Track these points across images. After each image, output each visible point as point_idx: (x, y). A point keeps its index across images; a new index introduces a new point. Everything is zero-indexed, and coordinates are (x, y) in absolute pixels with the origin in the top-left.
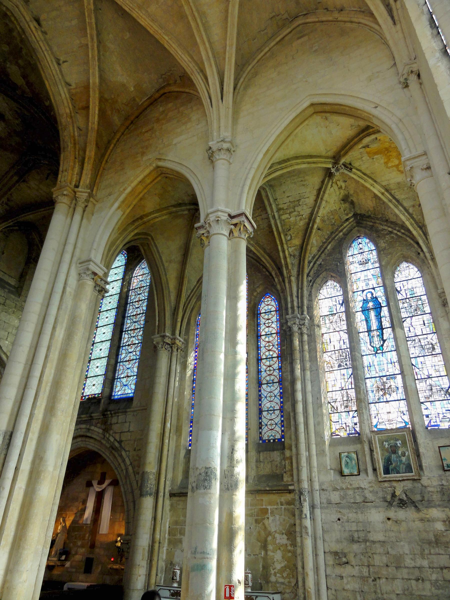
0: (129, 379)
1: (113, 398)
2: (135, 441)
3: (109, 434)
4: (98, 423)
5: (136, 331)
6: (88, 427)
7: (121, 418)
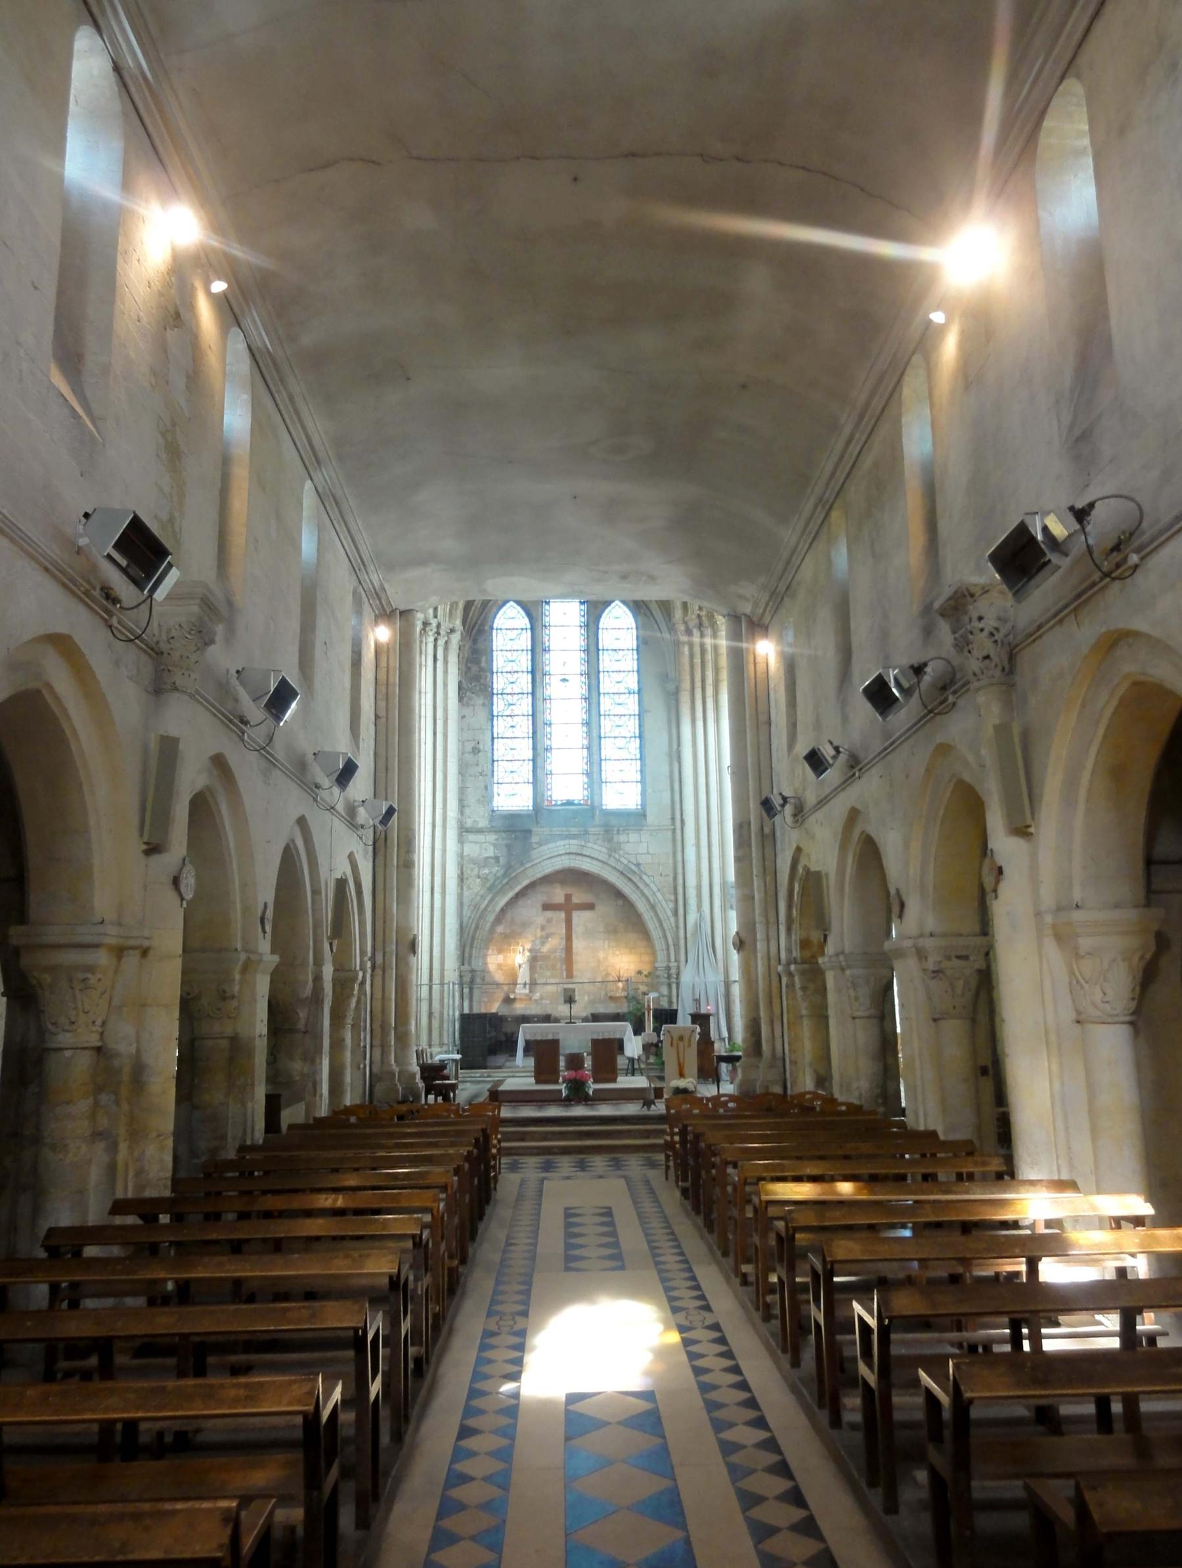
1: (604, 807)
2: (659, 865)
4: (598, 839)
6: (583, 843)
7: (633, 837)
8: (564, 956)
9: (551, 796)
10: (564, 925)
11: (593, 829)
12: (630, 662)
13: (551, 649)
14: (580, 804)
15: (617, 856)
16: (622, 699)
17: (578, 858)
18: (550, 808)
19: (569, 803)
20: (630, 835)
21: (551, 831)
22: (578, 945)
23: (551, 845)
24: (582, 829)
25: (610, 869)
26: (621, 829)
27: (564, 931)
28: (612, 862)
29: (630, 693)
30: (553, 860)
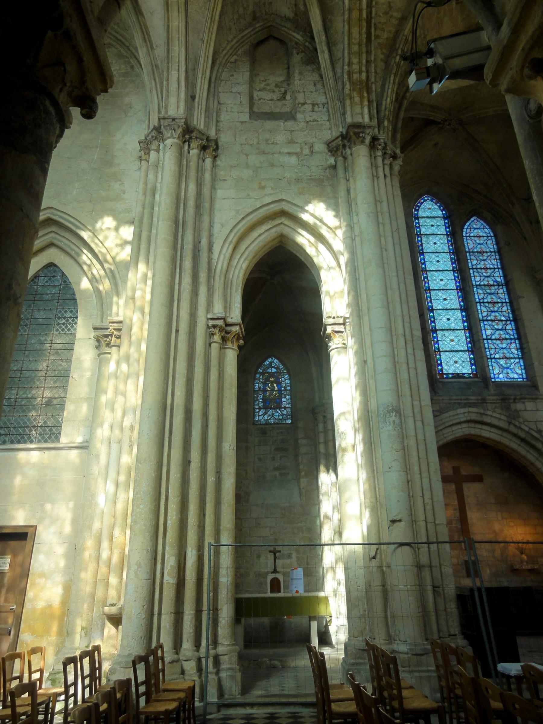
0: (508, 361)
3: (519, 422)
4: (495, 408)
5: (496, 305)
6: (482, 411)
7: (530, 405)
8: (460, 527)
9: (442, 370)
10: (455, 496)
11: (490, 398)
12: (494, 262)
13: (424, 251)
14: (470, 377)
15: (517, 423)
16: (493, 289)
17: (478, 426)
18: (441, 380)
19: (457, 376)
20: (526, 403)
21: (451, 399)
22: (473, 516)
23: (452, 413)
24: (480, 398)
25: (509, 436)
26: (518, 397)
27: (456, 502)
28: (512, 429)
29: (499, 285)
30: (454, 428)
